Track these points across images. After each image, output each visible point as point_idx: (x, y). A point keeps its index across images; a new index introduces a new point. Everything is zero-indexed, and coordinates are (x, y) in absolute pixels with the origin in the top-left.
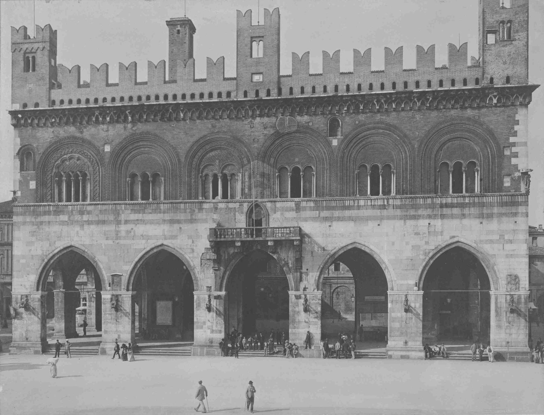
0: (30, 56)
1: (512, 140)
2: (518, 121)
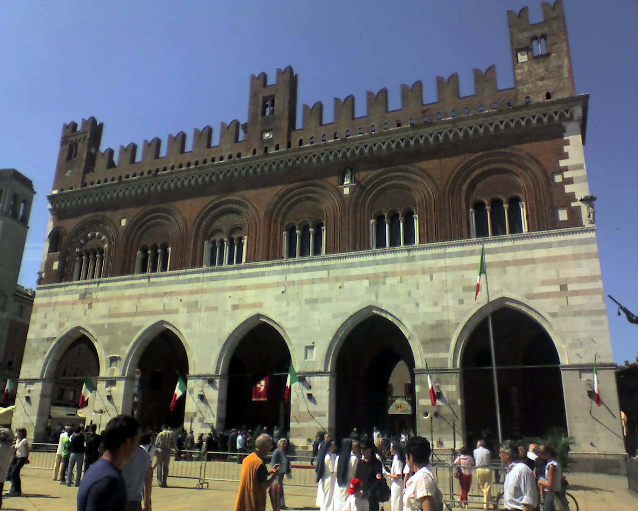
1: (563, 163)
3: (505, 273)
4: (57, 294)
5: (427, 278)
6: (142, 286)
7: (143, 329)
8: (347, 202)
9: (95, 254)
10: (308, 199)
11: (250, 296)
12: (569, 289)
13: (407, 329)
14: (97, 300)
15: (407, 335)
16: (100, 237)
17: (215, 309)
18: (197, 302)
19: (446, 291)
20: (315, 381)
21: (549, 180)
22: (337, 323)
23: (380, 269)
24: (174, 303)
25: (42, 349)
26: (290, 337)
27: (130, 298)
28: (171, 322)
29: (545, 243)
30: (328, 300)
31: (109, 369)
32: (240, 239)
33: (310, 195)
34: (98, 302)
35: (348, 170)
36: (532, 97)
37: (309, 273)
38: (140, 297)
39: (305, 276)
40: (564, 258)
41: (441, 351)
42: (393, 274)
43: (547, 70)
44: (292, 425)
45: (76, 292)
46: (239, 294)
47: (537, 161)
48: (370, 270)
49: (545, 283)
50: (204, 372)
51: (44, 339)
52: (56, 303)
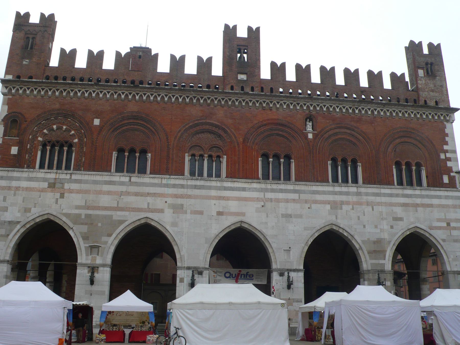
0: (31, 36)
1: (445, 147)
2: (447, 134)
3: (417, 211)
4: (18, 179)
5: (370, 208)
6: (122, 184)
7: (127, 223)
9: (62, 146)
10: (278, 135)
11: (233, 206)
12: (451, 226)
14: (71, 191)
15: (357, 246)
16: (68, 131)
17: (201, 213)
18: (182, 205)
19: (382, 219)
20: (292, 274)
21: (439, 156)
22: (309, 233)
23: (338, 198)
24: (159, 203)
26: (270, 242)
27: (109, 193)
28: (156, 219)
29: (438, 196)
30: (300, 216)
31: (90, 257)
32: (219, 157)
33: (281, 133)
35: (308, 120)
36: (428, 102)
37: (284, 194)
39: (281, 196)
41: (381, 259)
42: (348, 203)
43: (435, 86)
45: (44, 180)
46: (223, 202)
47: (432, 143)
48: (330, 198)
49: (439, 220)
51: (5, 222)
52: (17, 188)
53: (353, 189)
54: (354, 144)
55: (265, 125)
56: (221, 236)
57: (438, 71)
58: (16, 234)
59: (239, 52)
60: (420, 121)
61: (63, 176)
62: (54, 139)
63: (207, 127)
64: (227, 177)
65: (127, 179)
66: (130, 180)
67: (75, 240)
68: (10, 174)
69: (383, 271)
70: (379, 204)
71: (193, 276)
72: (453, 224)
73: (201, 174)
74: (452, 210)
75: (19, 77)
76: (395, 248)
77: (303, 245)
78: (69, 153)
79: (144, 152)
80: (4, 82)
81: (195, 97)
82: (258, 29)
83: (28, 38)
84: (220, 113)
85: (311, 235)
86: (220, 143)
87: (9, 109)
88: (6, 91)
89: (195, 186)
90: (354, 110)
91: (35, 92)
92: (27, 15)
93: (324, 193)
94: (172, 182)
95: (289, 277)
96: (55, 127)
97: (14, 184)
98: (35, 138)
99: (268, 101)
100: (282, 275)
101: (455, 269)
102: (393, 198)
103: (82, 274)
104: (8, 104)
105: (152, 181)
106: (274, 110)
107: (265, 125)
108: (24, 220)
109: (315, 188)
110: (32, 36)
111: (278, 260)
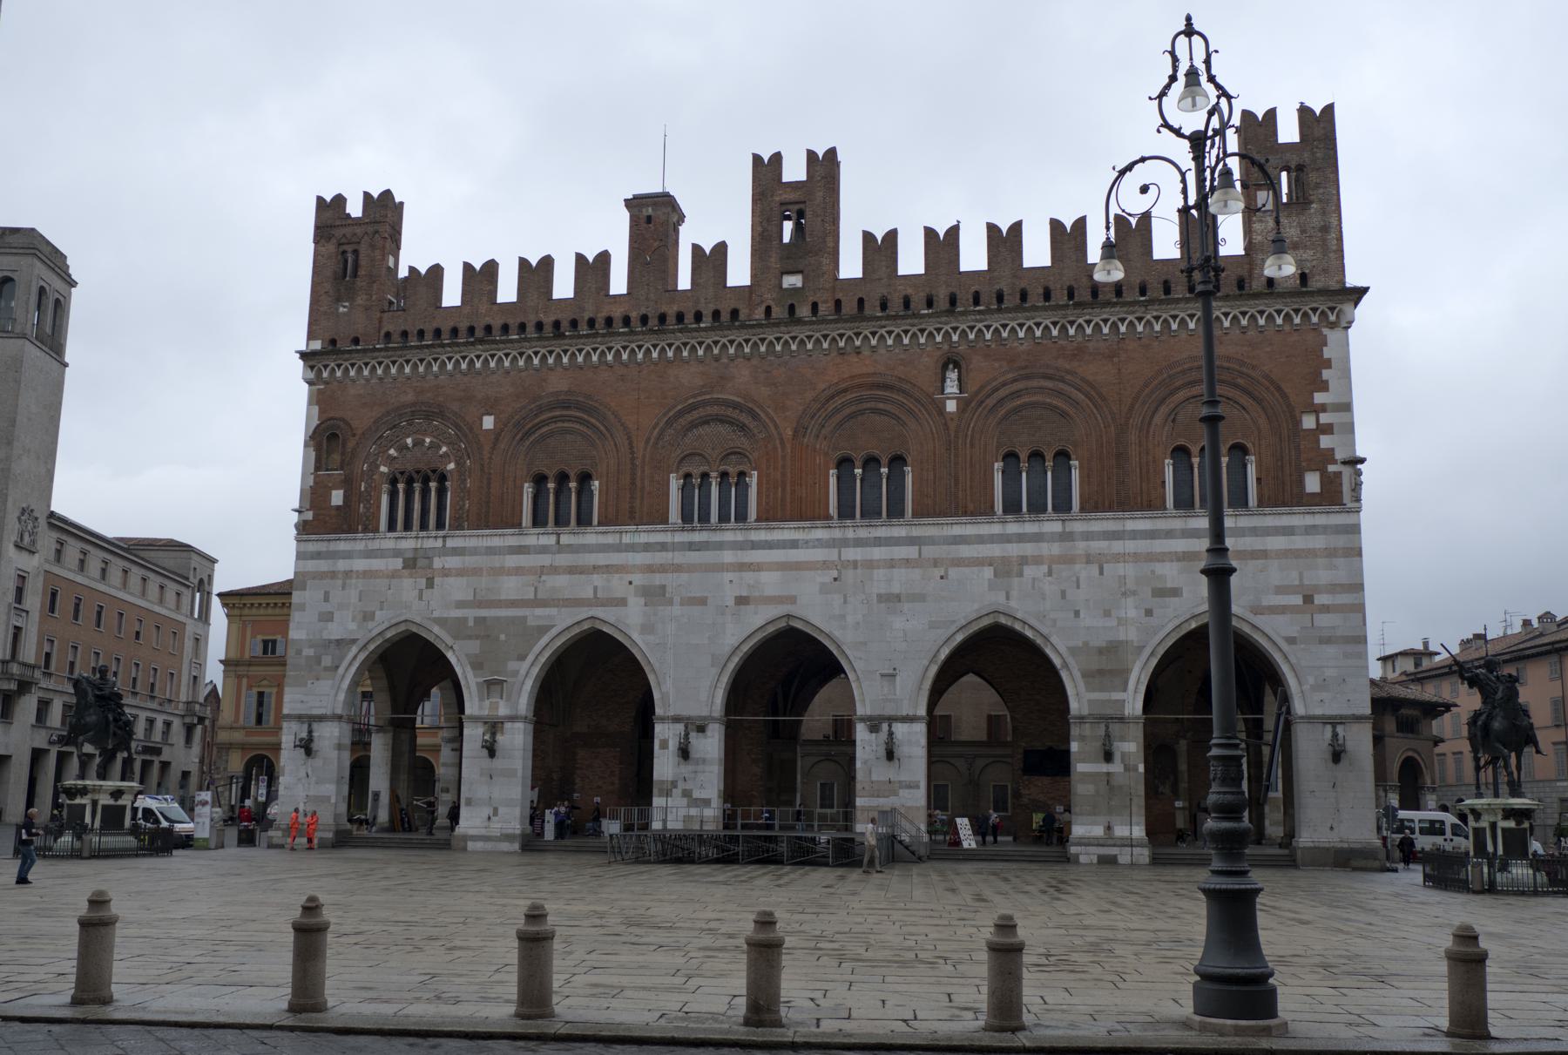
0: (349, 248)
1: (1319, 398)
2: (1329, 360)
4: (348, 555)
5: (1095, 569)
6: (544, 550)
7: (554, 632)
8: (952, 426)
9: (426, 480)
10: (875, 411)
11: (770, 582)
13: (1059, 649)
14: (446, 573)
15: (1057, 661)
16: (435, 446)
17: (702, 601)
18: (663, 587)
19: (1124, 594)
20: (900, 729)
23: (1014, 550)
24: (617, 585)
25: (327, 661)
29: (1284, 528)
30: (921, 598)
31: (487, 703)
32: (742, 474)
33: (881, 406)
34: (446, 575)
38: (542, 571)
39: (878, 553)
40: (1311, 553)
41: (1114, 689)
42: (1037, 560)
43: (1303, 231)
44: (859, 802)
45: (397, 553)
46: (749, 576)
47: (1279, 388)
48: (995, 550)
49: (1281, 590)
50: (685, 713)
51: (330, 641)
52: (348, 574)
53: (1056, 527)
54: (1064, 414)
55: (845, 391)
56: (746, 648)
57: (1318, 186)
58: (350, 664)
59: (788, 218)
60: (1251, 333)
61: (430, 543)
62: (409, 467)
63: (715, 410)
64: (758, 520)
65: (552, 540)
66: (558, 542)
67: (458, 670)
68: (334, 546)
69: (1121, 719)
70: (1118, 558)
71: (687, 735)
72: (1320, 599)
73: (704, 518)
74: (1321, 561)
75: (333, 342)
76: (1154, 662)
77: (926, 662)
78: (441, 492)
79: (585, 478)
80: (304, 356)
81: (685, 344)
82: (832, 153)
83: (344, 252)
84: (742, 375)
85: (944, 638)
86: (743, 442)
87: (321, 412)
88: (311, 375)
89: (691, 543)
90: (1064, 329)
91: (366, 373)
92: (340, 200)
93: (980, 540)
94: (644, 538)
95: (891, 734)
96: (409, 441)
97: (342, 565)
98: (374, 467)
99: (850, 333)
100: (874, 729)
101: (1318, 711)
102: (1157, 542)
103: (473, 735)
104: (318, 403)
105: (602, 539)
106: (866, 352)
107: (845, 391)
108: (363, 637)
109: (957, 530)
110: (355, 242)
111: (868, 697)
